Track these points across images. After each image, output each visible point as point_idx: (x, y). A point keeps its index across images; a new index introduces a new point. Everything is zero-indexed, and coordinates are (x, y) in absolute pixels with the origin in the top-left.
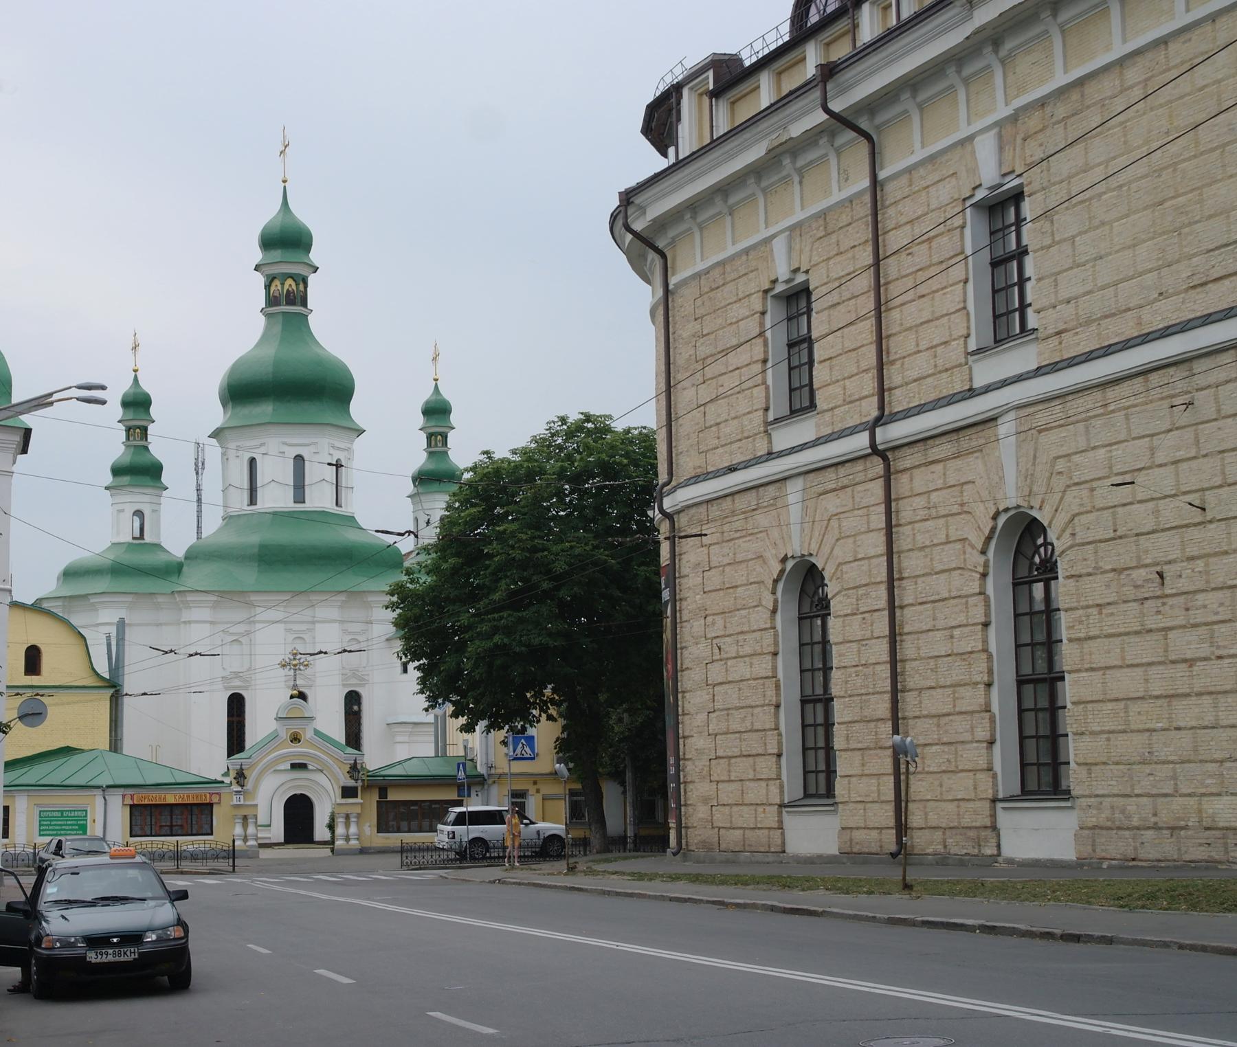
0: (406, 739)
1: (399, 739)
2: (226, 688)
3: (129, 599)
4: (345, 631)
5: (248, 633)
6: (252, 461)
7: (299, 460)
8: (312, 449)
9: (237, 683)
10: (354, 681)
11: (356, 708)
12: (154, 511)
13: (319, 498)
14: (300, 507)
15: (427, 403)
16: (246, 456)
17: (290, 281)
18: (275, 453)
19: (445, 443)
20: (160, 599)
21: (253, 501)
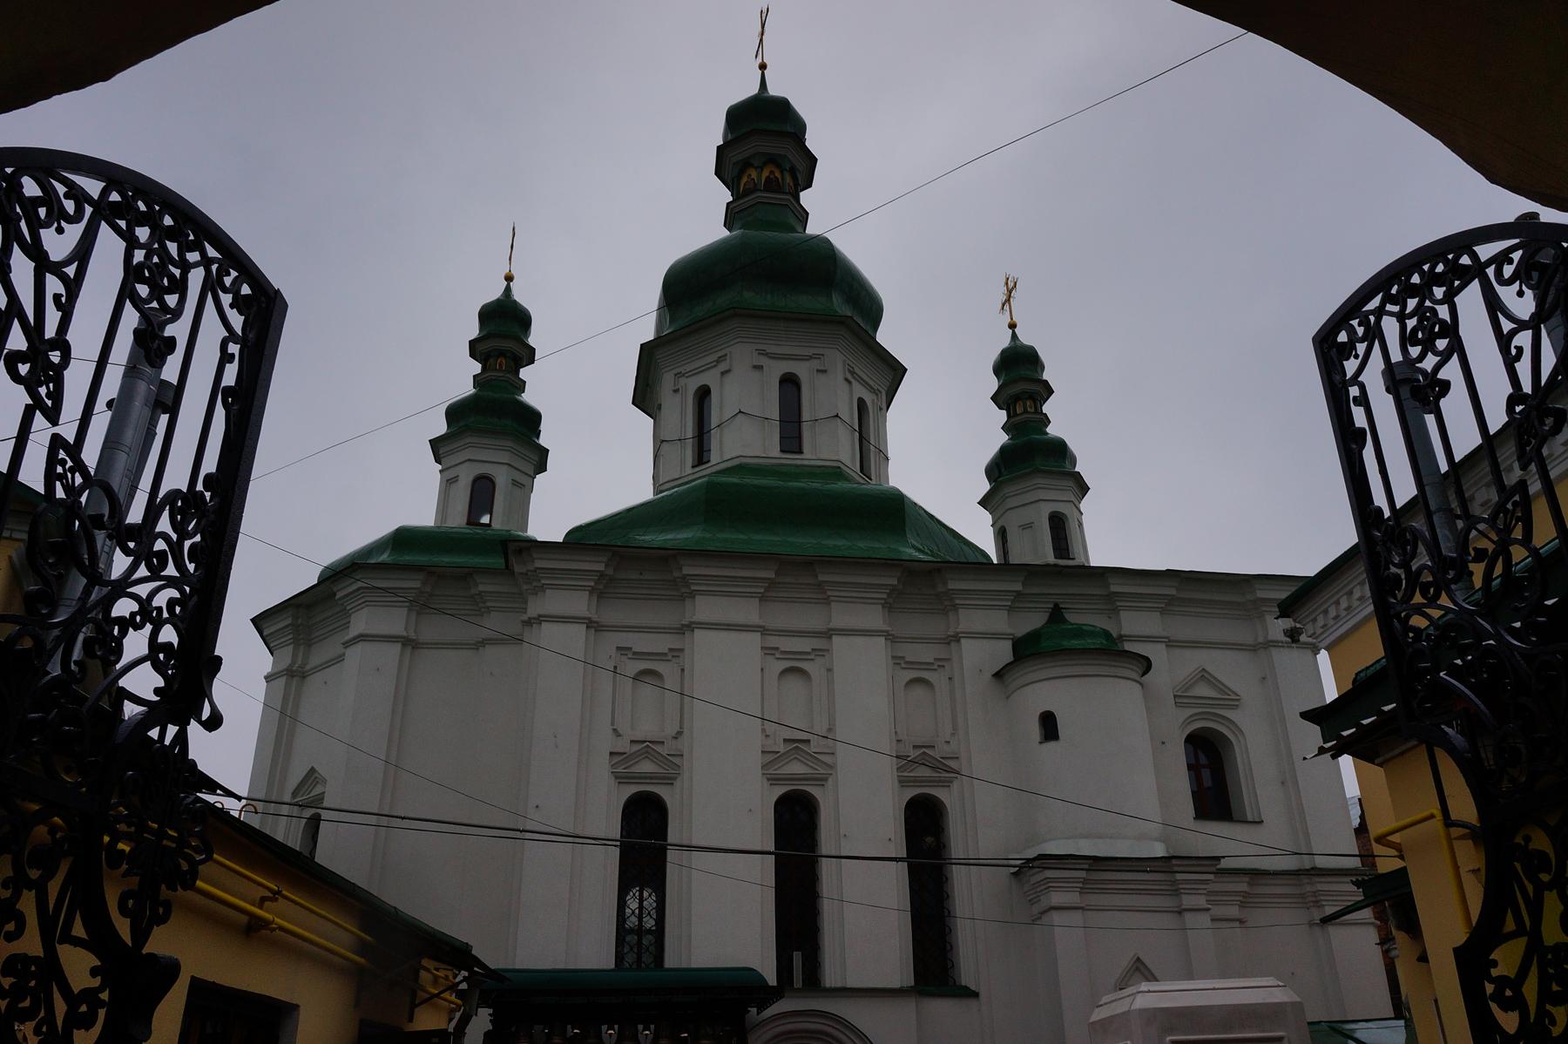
0: (1071, 898)
1: (1057, 898)
3: (413, 583)
4: (898, 661)
5: (676, 653)
6: (703, 394)
7: (790, 384)
8: (815, 364)
9: (647, 767)
12: (515, 483)
13: (829, 446)
14: (791, 459)
15: (1003, 352)
16: (693, 384)
20: (484, 586)
21: (701, 457)
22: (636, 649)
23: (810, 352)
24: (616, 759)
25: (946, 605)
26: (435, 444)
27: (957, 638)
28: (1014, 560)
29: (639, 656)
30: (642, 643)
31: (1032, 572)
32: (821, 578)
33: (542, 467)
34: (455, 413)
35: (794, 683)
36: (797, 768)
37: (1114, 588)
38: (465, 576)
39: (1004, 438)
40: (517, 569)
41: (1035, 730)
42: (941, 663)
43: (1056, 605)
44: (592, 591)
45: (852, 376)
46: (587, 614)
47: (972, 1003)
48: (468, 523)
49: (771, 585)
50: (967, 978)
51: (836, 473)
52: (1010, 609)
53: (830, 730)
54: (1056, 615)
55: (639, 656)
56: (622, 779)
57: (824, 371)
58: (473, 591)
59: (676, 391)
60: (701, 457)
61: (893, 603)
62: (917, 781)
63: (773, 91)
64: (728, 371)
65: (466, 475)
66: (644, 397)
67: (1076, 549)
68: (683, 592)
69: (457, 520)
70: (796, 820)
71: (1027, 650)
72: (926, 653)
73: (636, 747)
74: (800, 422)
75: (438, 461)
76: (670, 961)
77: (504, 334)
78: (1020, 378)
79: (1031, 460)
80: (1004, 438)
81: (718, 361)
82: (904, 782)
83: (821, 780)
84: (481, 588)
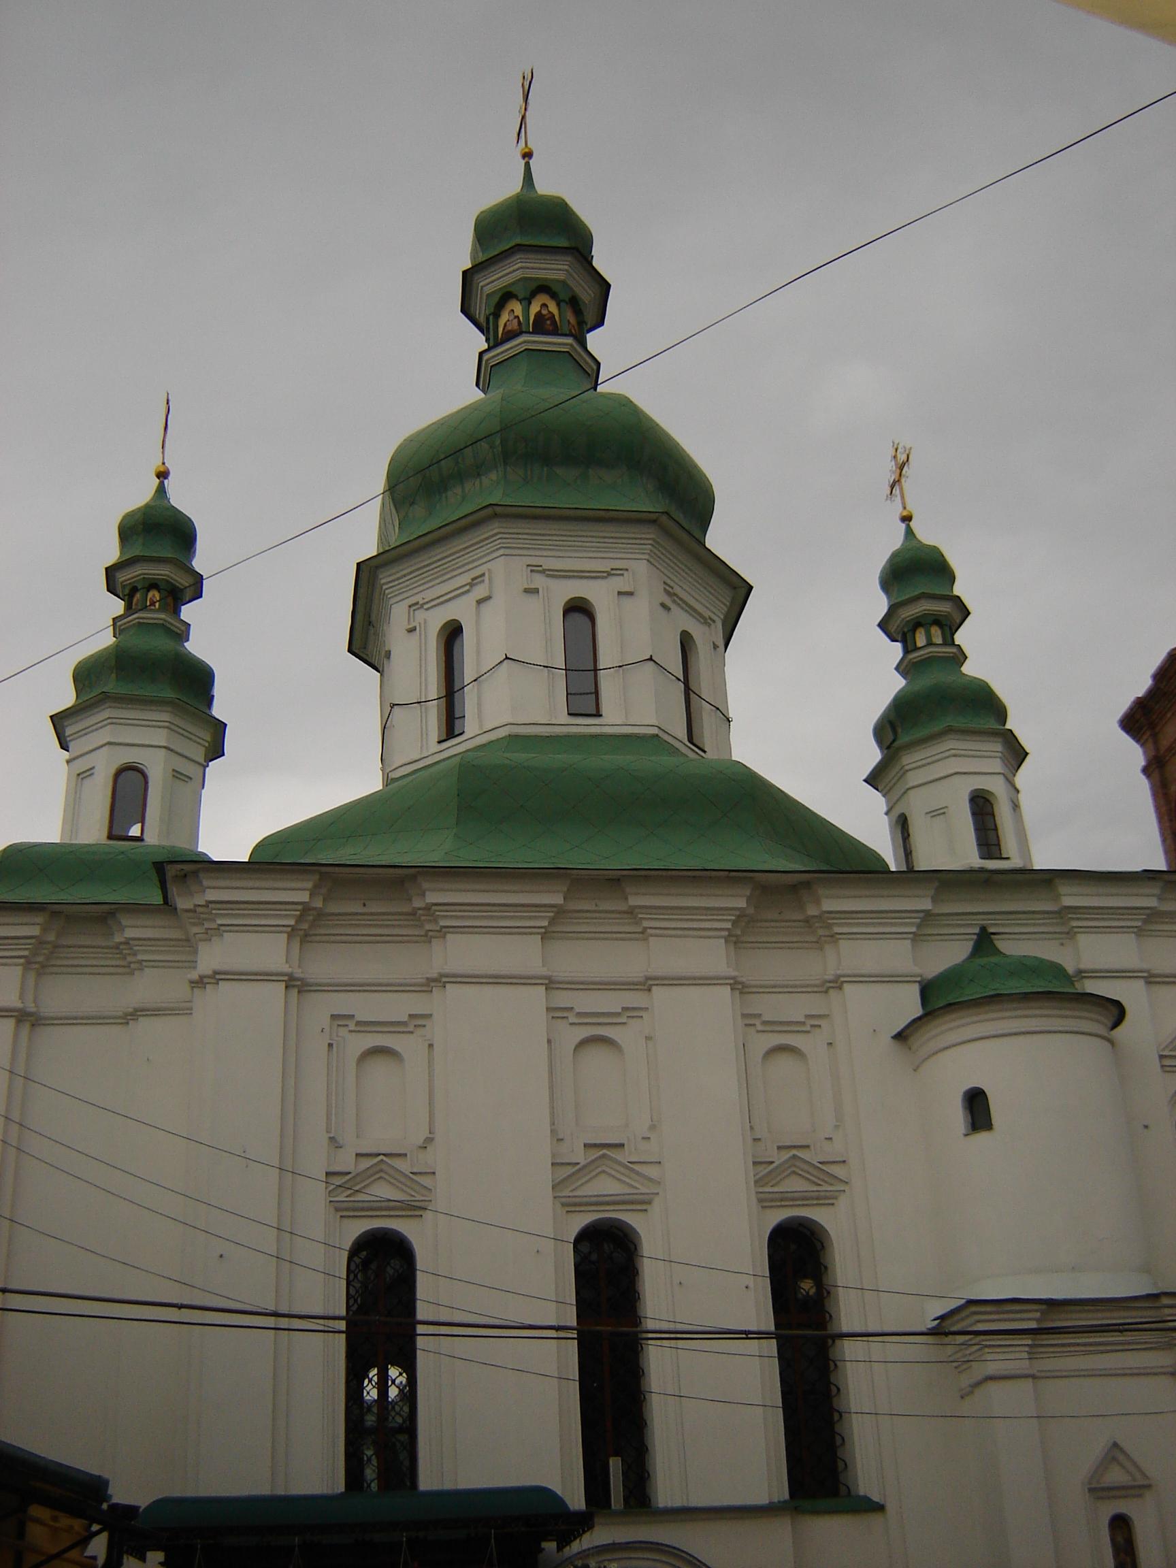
2: (345, 1211)
4: (749, 1020)
5: (418, 1020)
6: (452, 634)
7: (578, 609)
8: (618, 583)
10: (795, 1185)
11: (807, 1286)
12: (177, 775)
13: (636, 704)
15: (895, 555)
16: (436, 620)
17: (542, 298)
18: (506, 607)
19: (949, 641)
20: (133, 929)
21: (451, 726)
22: (360, 1017)
23: (605, 566)
24: (338, 1181)
25: (821, 933)
26: (58, 720)
27: (837, 984)
28: (922, 864)
29: (366, 1026)
30: (365, 1007)
31: (948, 882)
32: (634, 901)
33: (216, 751)
34: (87, 675)
35: (597, 1058)
36: (605, 1186)
37: (1068, 901)
38: (105, 917)
39: (899, 682)
40: (182, 903)
41: (958, 1116)
42: (813, 1022)
43: (983, 929)
44: (292, 932)
45: (671, 600)
46: (286, 969)
47: (875, 1519)
48: (111, 837)
49: (559, 913)
50: (866, 1483)
51: (653, 742)
52: (916, 938)
53: (653, 1127)
54: (984, 942)
55: (366, 1026)
56: (345, 1211)
57: (631, 594)
58: (118, 939)
59: (411, 630)
60: (451, 726)
61: (741, 933)
62: (784, 1199)
63: (545, 187)
64: (489, 598)
65: (105, 766)
66: (365, 641)
67: (1009, 844)
68: (427, 927)
69: (93, 832)
70: (606, 1264)
71: (940, 999)
72: (794, 1008)
73: (366, 1164)
74: (596, 670)
75: (64, 746)
76: (427, 1480)
77: (158, 556)
78: (920, 596)
79: (941, 714)
80: (899, 682)
81: (473, 583)
82: (765, 1202)
83: (642, 1203)
84: (130, 933)
